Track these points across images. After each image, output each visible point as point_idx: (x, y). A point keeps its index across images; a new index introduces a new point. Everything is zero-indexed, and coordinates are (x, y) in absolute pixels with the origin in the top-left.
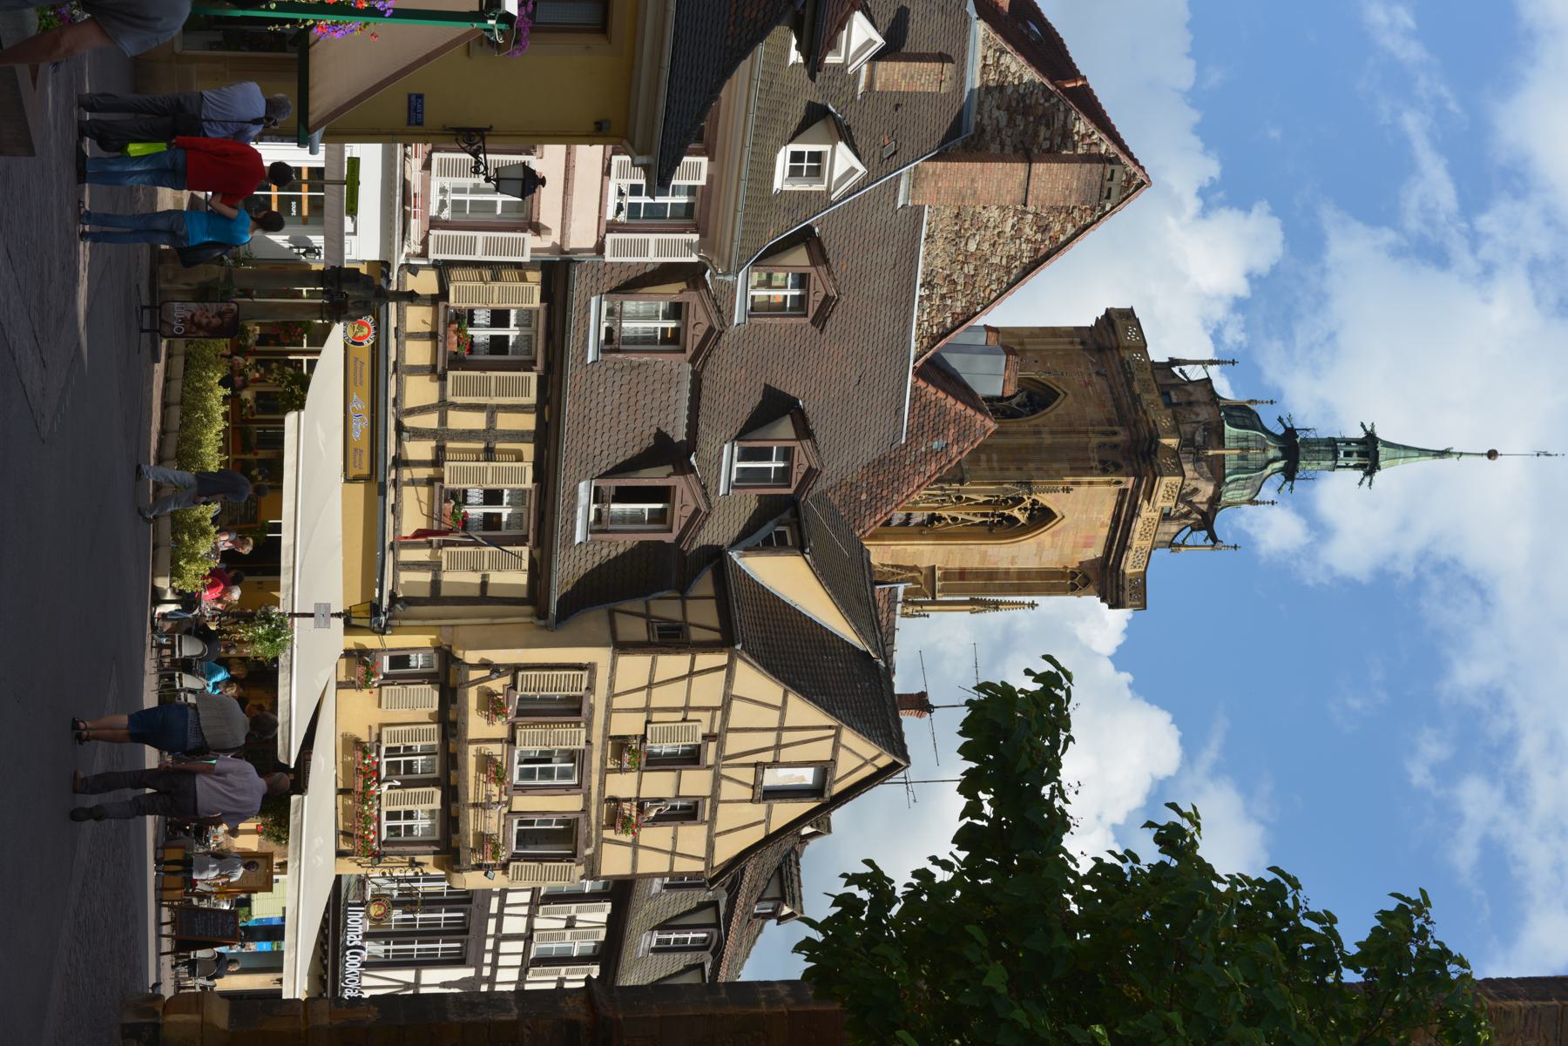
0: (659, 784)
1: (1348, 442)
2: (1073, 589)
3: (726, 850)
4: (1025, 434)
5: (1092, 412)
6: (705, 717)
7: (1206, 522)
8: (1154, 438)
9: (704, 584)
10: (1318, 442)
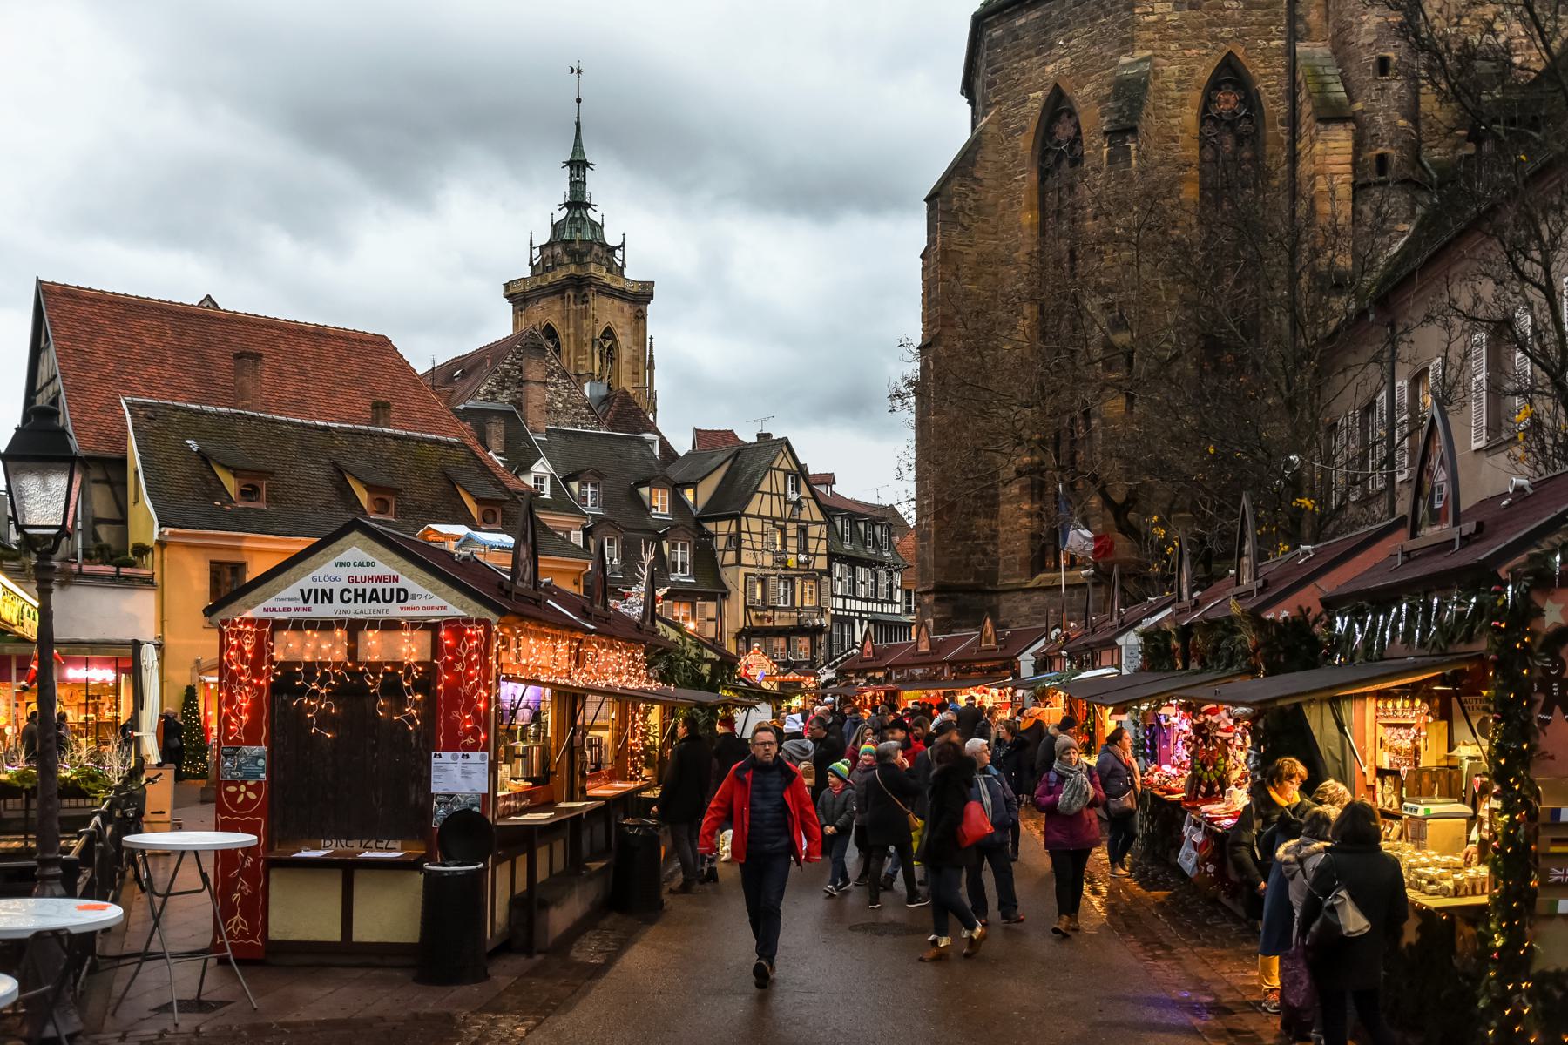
0: (792, 544)
1: (572, 175)
2: (644, 317)
3: (818, 516)
5: (557, 307)
6: (766, 526)
7: (612, 250)
8: (571, 277)
9: (710, 527)
10: (571, 191)
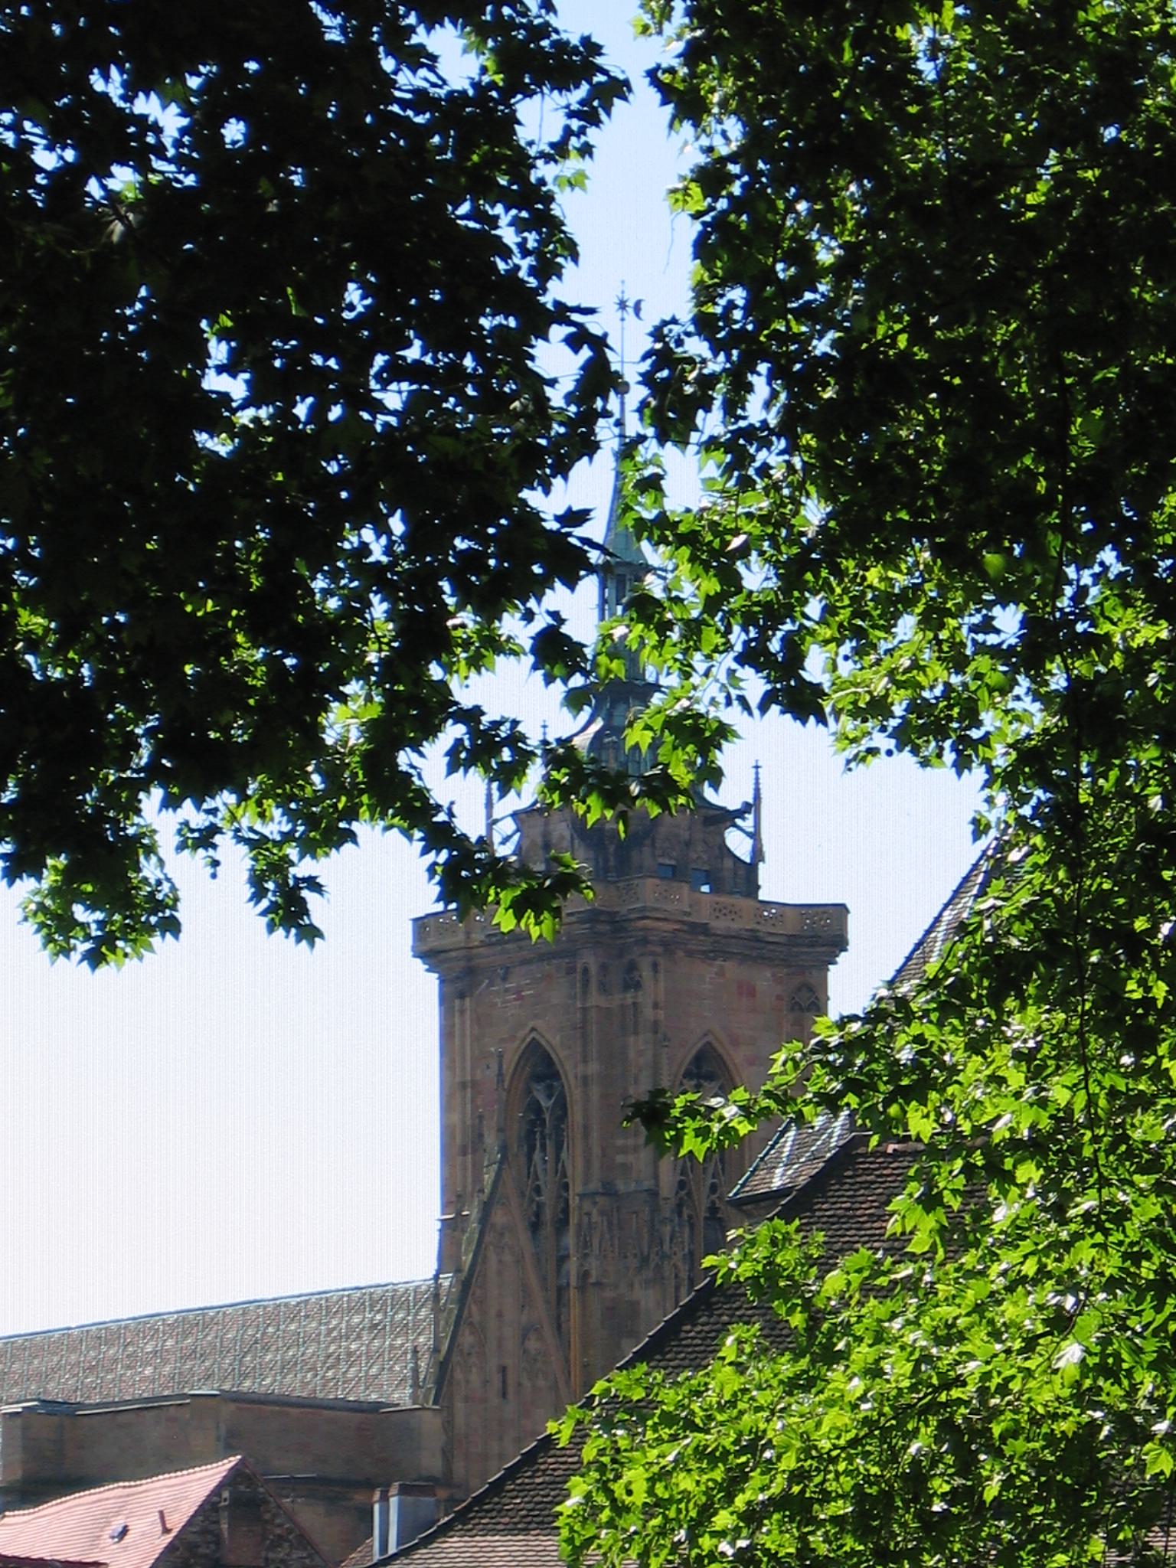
4: (586, 1099)
